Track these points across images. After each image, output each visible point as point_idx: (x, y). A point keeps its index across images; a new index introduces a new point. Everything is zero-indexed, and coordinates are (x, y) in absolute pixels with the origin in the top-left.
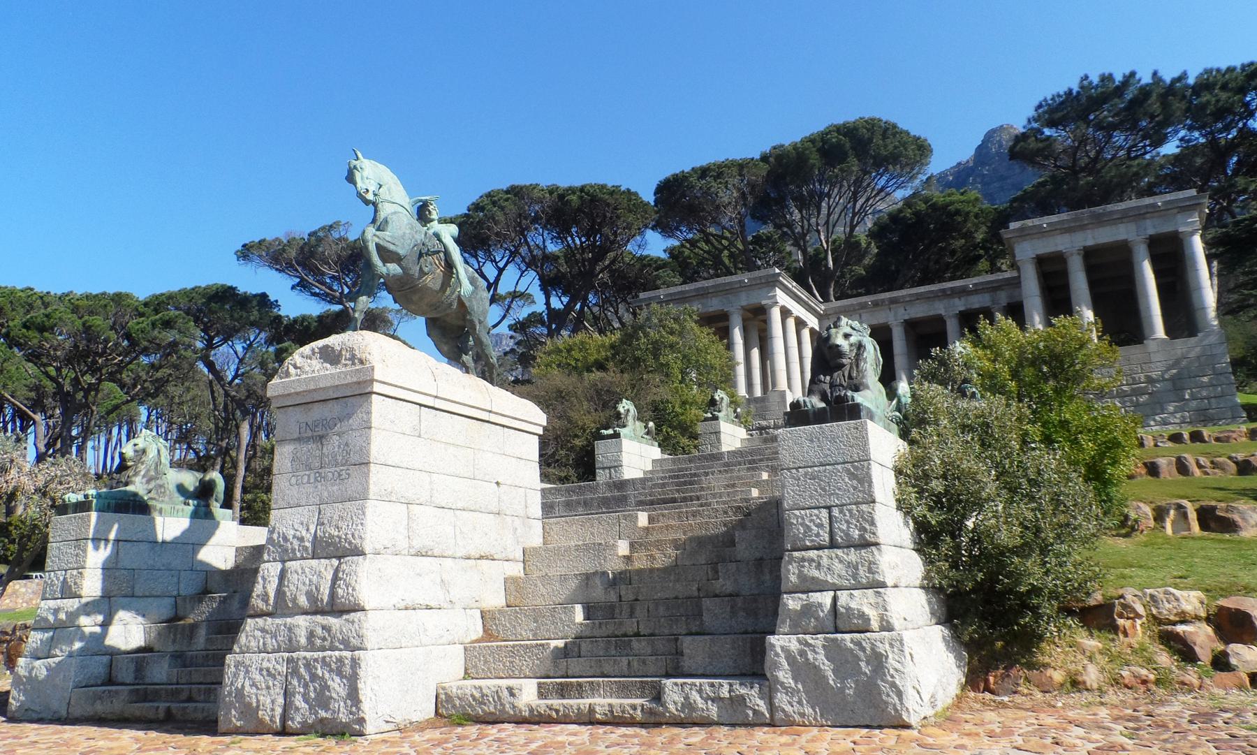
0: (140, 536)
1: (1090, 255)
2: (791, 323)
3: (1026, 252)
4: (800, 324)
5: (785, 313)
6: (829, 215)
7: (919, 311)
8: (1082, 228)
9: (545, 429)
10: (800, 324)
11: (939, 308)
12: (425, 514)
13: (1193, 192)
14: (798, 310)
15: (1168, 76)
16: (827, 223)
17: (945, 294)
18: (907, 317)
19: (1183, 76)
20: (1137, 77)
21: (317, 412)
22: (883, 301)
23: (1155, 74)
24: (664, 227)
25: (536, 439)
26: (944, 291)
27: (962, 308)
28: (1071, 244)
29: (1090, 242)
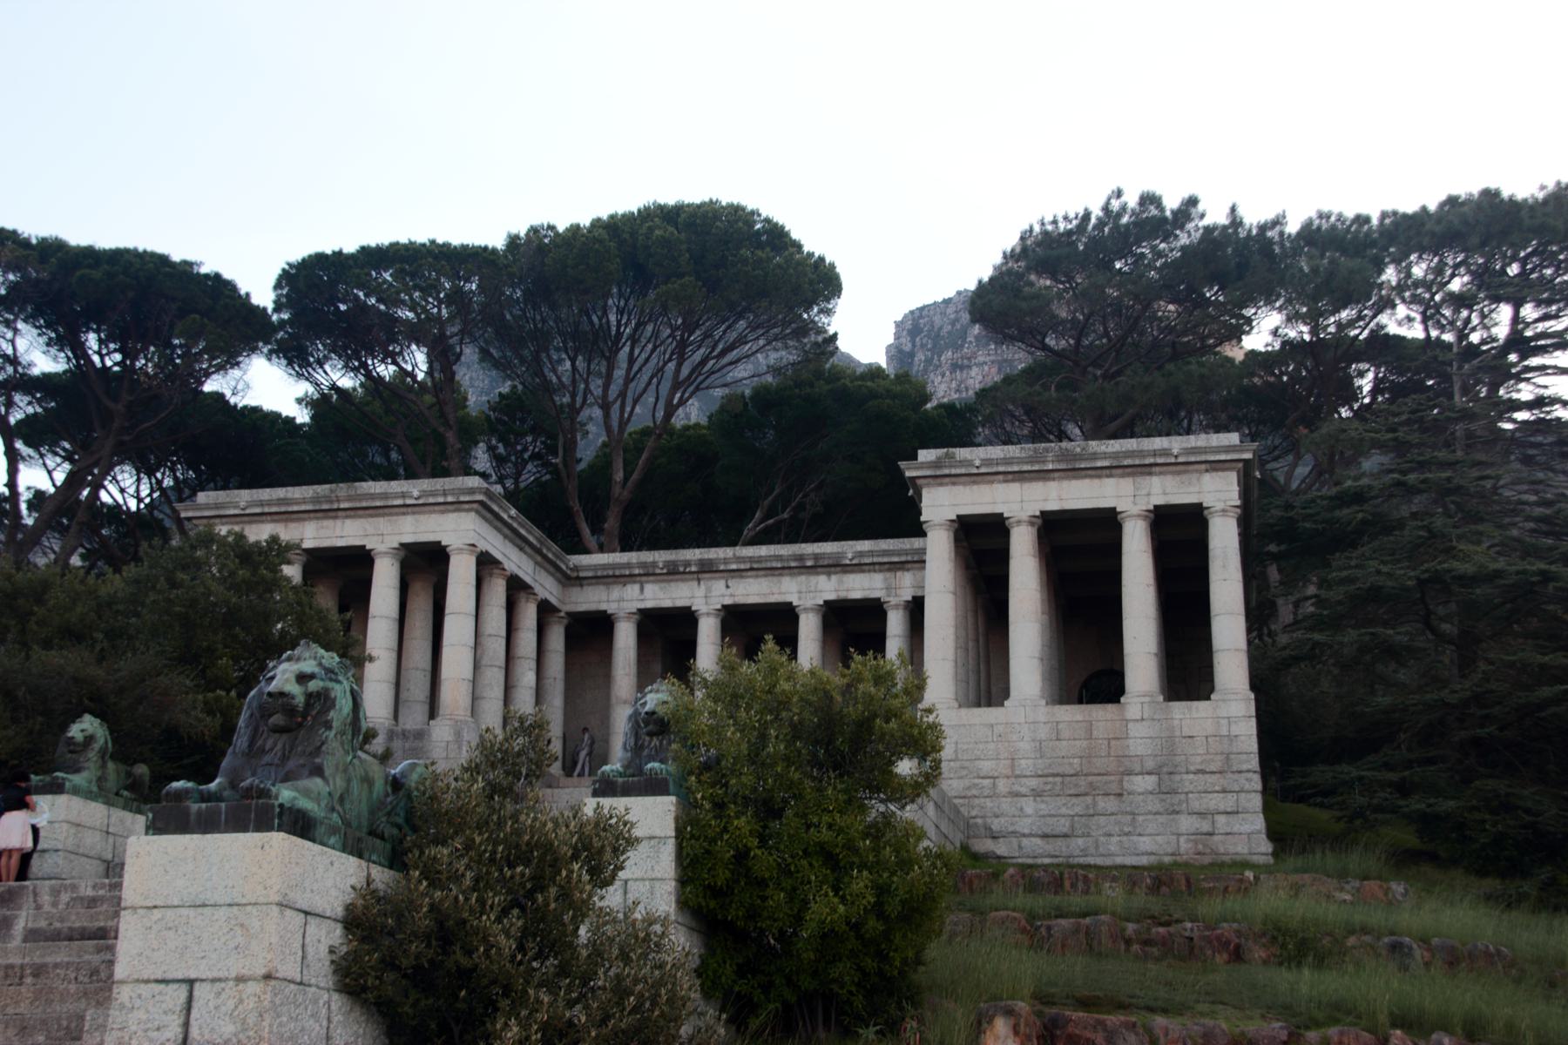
1: (1051, 526)
2: (497, 592)
3: (941, 505)
4: (516, 587)
5: (486, 563)
6: (628, 380)
7: (753, 591)
8: (1043, 475)
10: (516, 587)
11: (787, 590)
13: (1233, 438)
14: (515, 561)
15: (1253, 217)
16: (622, 395)
17: (803, 567)
18: (728, 601)
19: (1277, 222)
20: (1201, 207)
22: (687, 563)
23: (1233, 209)
24: (296, 356)
26: (801, 558)
27: (832, 596)
28: (1021, 503)
29: (1053, 506)
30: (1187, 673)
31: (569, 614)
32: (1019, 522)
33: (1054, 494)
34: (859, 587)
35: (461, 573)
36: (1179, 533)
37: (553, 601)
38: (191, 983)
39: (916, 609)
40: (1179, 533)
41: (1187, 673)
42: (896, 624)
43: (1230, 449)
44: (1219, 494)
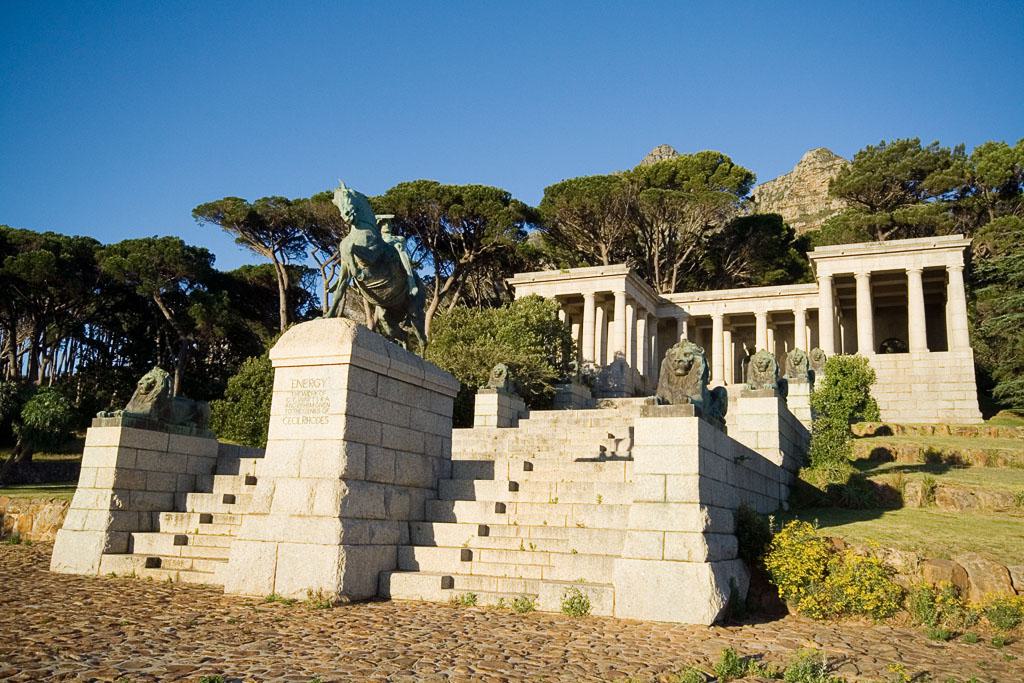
0: (153, 446)
1: (875, 277)
9: (459, 394)
12: (377, 453)
21: (307, 373)
25: (451, 402)
29: (876, 269)
30: (937, 340)
31: (661, 319)
32: (861, 276)
33: (877, 264)
34: (781, 305)
35: (620, 301)
36: (934, 279)
37: (653, 314)
38: (665, 475)
39: (812, 316)
40: (934, 279)
41: (937, 340)
42: (800, 321)
43: (958, 241)
44: (954, 263)
